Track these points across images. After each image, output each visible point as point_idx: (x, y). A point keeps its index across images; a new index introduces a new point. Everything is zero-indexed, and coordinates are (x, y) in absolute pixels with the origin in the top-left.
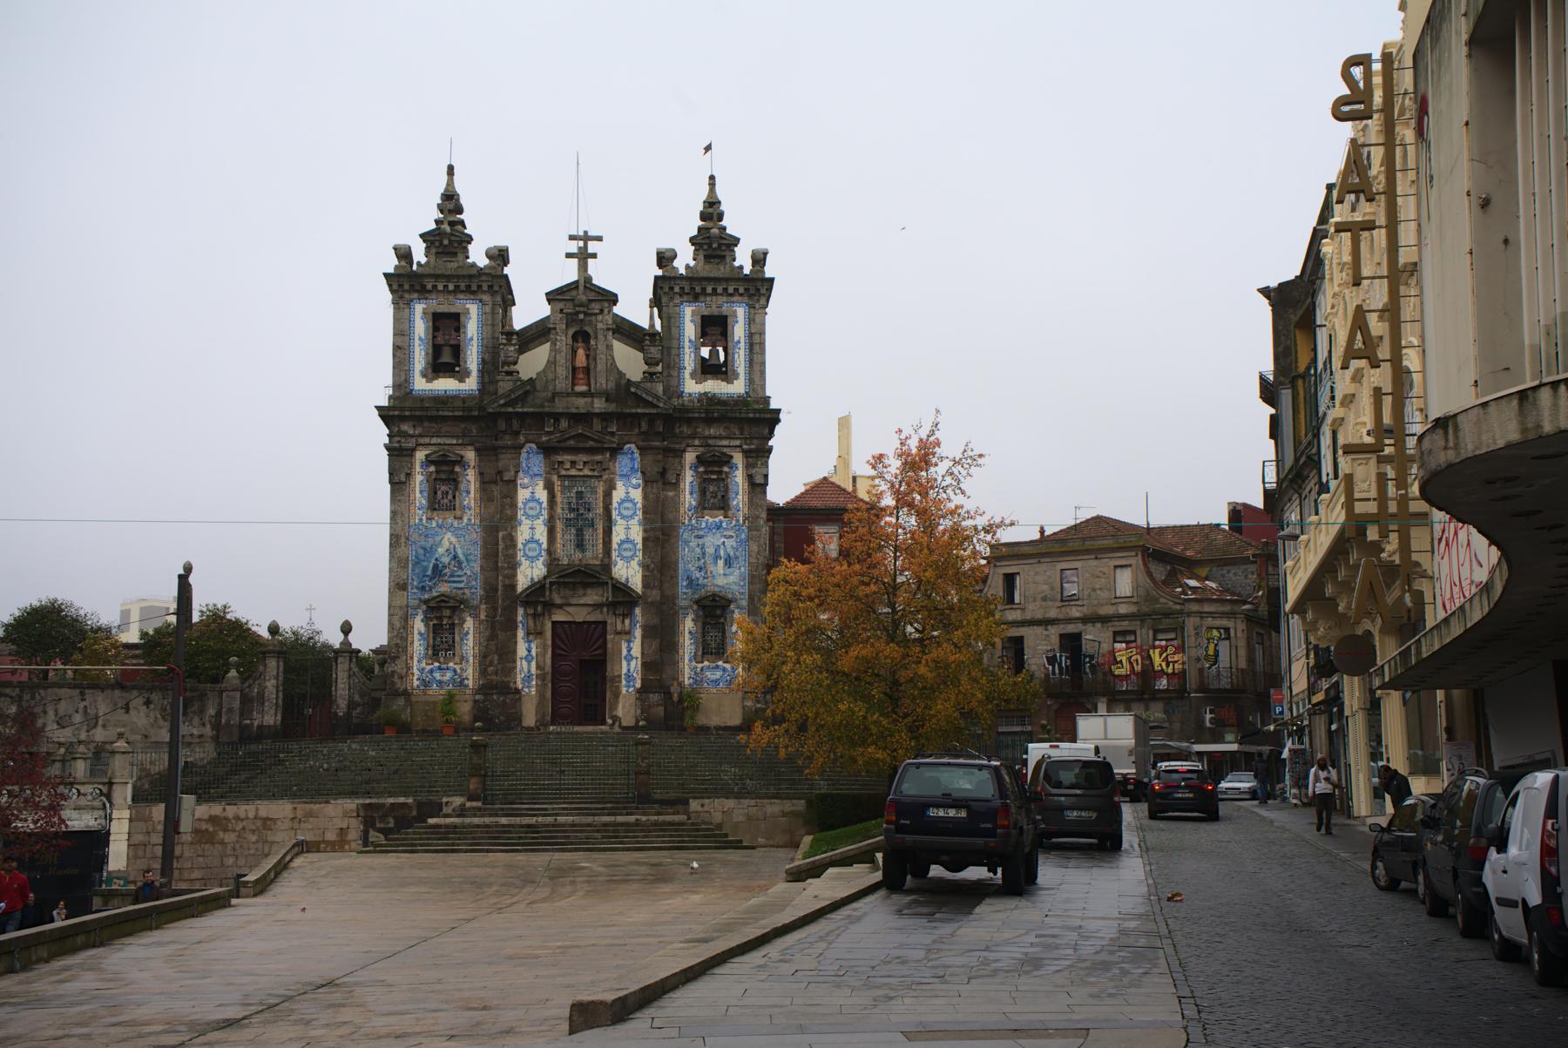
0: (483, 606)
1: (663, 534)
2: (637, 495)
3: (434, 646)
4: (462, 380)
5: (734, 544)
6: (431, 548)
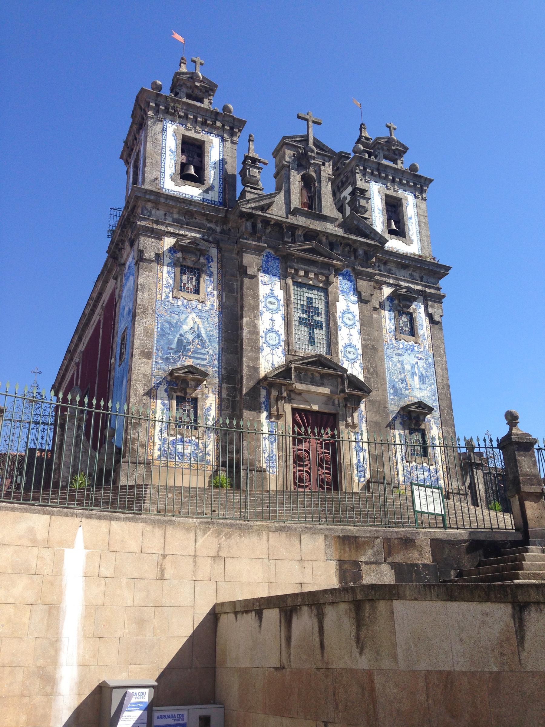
0: (225, 385)
2: (355, 308)
5: (425, 365)
6: (176, 324)
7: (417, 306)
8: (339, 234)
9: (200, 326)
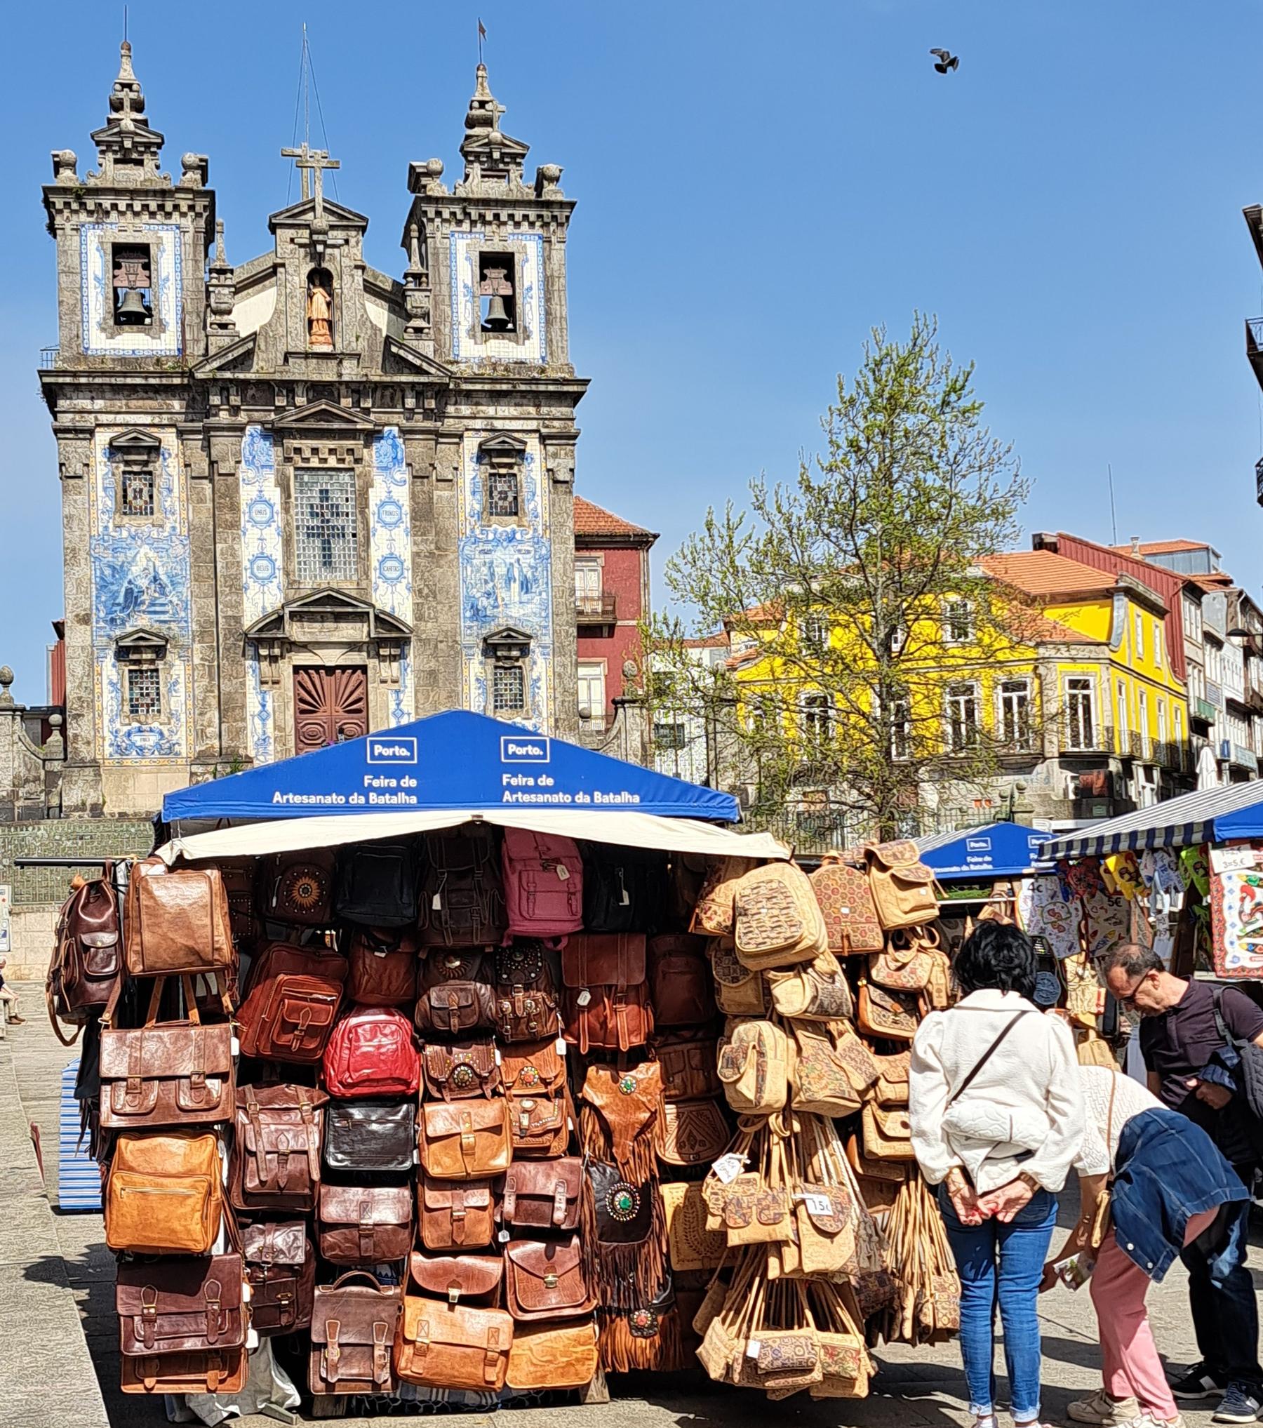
0: (197, 646)
1: (438, 548)
2: (402, 494)
3: (131, 700)
6: (122, 566)
9: (158, 564)
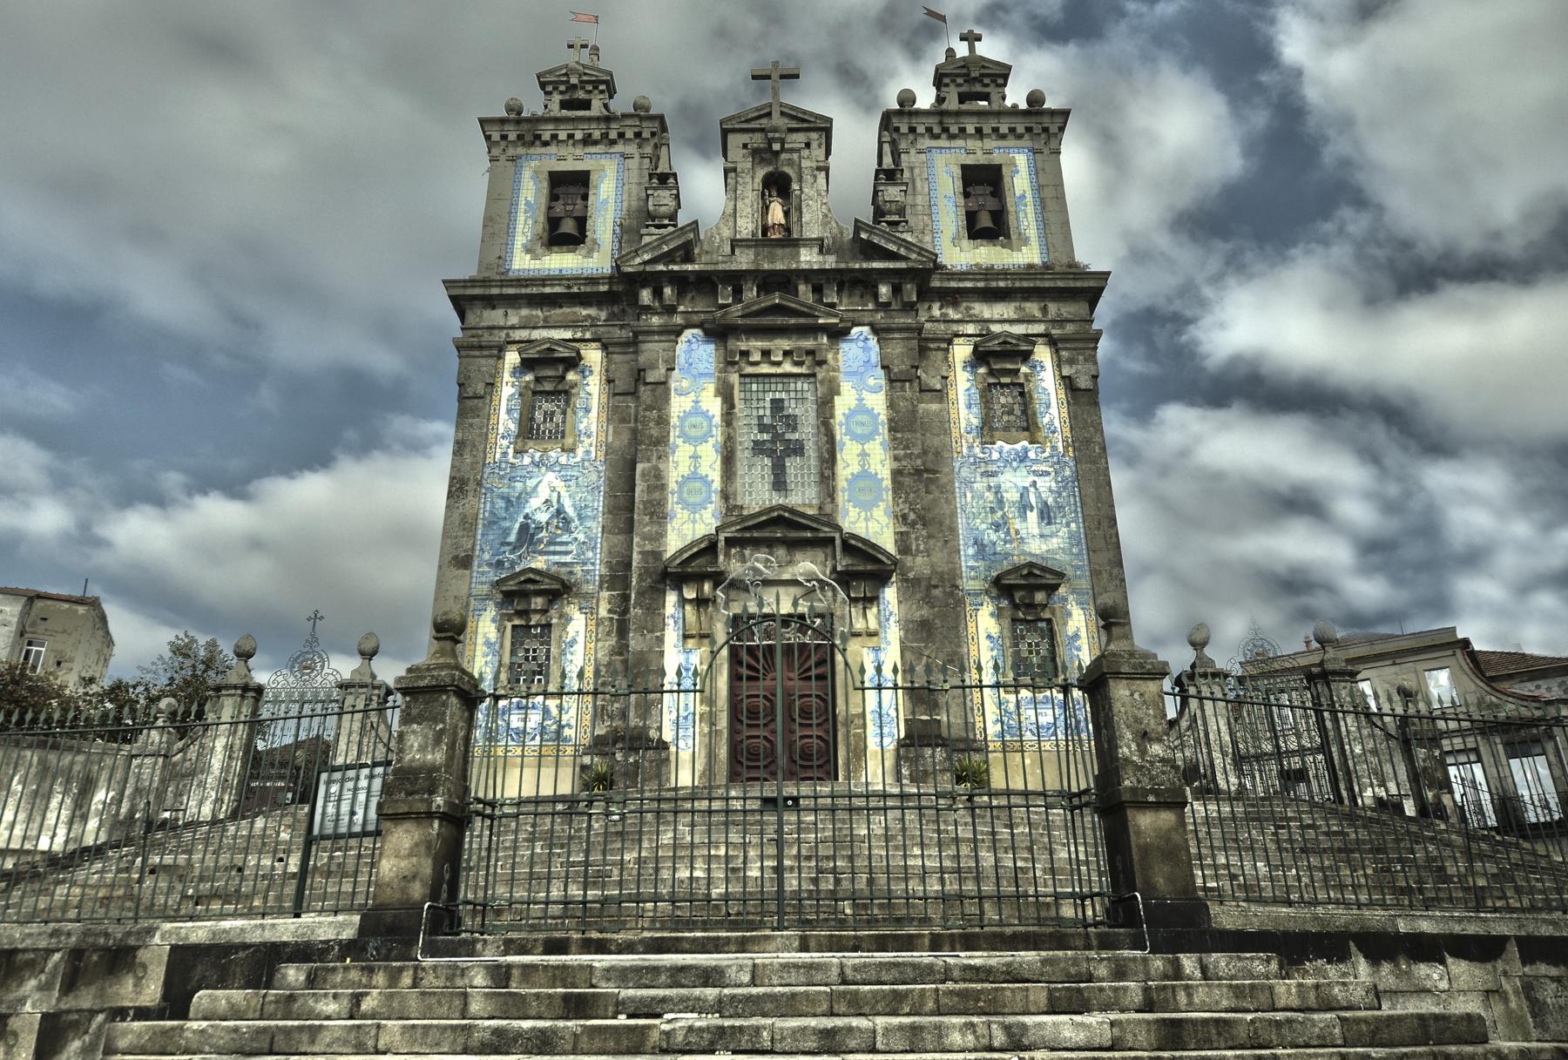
0: (605, 594)
2: (878, 403)
4: (589, 254)
5: (1053, 484)
6: (519, 498)
7: (1035, 367)
8: (827, 267)
9: (562, 494)
